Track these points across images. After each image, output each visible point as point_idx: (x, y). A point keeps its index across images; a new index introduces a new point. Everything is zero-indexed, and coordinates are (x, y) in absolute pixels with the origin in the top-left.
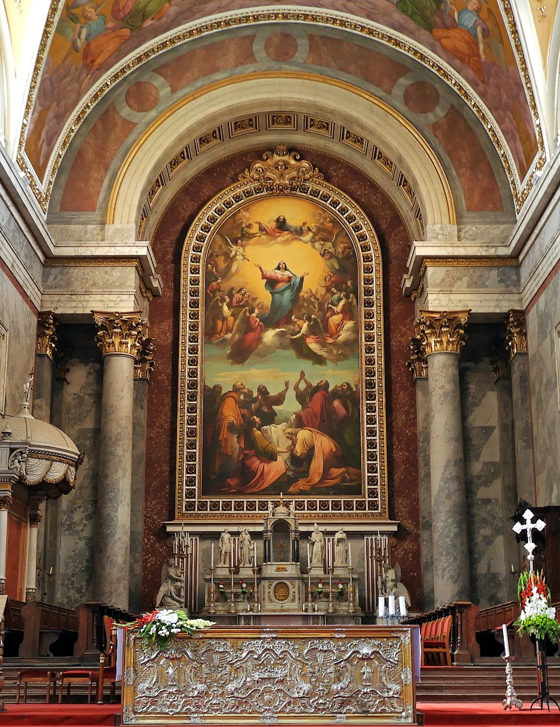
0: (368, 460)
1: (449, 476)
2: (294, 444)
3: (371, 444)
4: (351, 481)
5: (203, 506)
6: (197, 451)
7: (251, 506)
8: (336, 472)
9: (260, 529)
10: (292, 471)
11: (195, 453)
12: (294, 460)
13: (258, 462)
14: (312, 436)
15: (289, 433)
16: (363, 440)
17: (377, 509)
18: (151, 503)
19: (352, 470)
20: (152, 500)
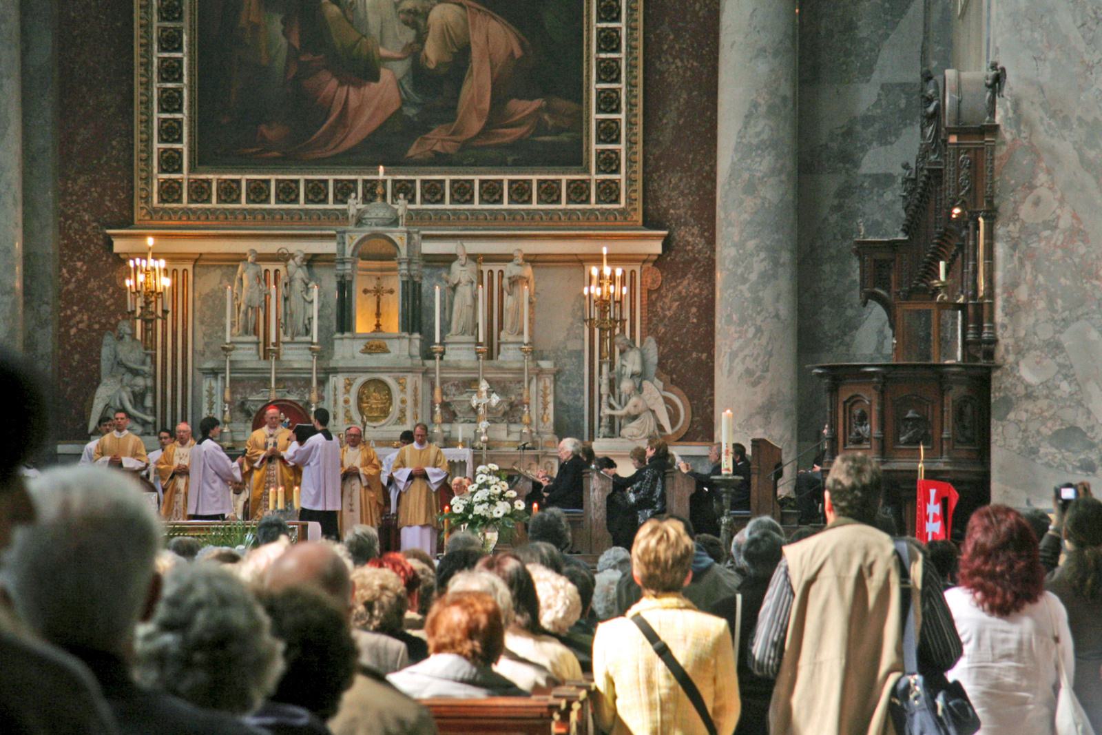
0: (599, 80)
1: (755, 141)
2: (421, 39)
3: (609, 41)
4: (558, 131)
5: (200, 191)
6: (184, 56)
7: (317, 191)
8: (522, 107)
9: (330, 247)
10: (415, 104)
11: (180, 61)
12: (420, 76)
13: (334, 83)
14: (466, 21)
15: (409, 11)
16: (589, 30)
17: (617, 201)
18: (75, 180)
19: (560, 103)
20: (79, 172)
